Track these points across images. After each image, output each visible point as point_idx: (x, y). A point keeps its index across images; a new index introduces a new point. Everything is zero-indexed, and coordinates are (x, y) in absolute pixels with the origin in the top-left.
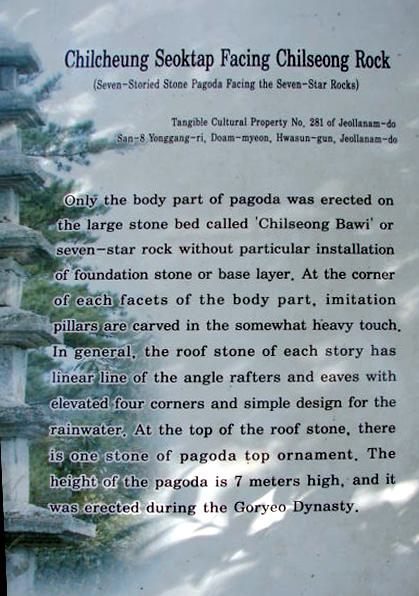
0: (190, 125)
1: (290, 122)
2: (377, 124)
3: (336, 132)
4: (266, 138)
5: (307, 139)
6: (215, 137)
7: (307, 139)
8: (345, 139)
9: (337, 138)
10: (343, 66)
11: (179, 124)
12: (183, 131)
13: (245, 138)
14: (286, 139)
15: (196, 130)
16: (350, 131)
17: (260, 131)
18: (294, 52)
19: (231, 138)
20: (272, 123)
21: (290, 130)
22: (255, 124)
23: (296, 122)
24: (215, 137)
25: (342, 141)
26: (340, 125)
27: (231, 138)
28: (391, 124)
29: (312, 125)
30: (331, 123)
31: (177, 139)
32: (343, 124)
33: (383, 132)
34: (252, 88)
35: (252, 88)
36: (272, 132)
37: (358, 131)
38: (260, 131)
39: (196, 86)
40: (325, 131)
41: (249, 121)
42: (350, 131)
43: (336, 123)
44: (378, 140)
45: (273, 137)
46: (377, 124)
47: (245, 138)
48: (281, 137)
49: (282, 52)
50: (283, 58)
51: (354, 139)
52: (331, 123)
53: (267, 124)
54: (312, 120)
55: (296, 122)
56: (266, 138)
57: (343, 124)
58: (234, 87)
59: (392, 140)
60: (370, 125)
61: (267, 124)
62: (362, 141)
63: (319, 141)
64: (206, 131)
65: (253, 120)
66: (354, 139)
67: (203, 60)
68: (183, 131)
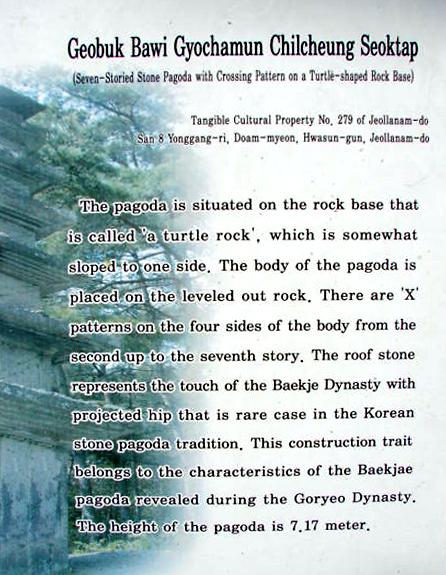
0: (210, 124)
2: (408, 121)
3: (366, 131)
4: (291, 138)
5: (336, 138)
6: (239, 138)
7: (336, 138)
8: (375, 139)
9: (366, 137)
11: (200, 123)
12: (203, 130)
13: (270, 138)
14: (314, 139)
15: (217, 130)
17: (284, 130)
19: (256, 138)
21: (317, 129)
22: (280, 122)
23: (324, 120)
24: (239, 138)
25: (372, 140)
27: (256, 138)
28: (423, 121)
29: (340, 123)
30: (361, 121)
31: (198, 140)
32: (374, 121)
33: (415, 130)
36: (298, 131)
37: (391, 130)
38: (284, 130)
40: (354, 129)
41: (274, 119)
43: (367, 120)
44: (409, 139)
45: (299, 137)
46: (408, 121)
47: (270, 138)
48: (308, 137)
52: (361, 121)
53: (293, 121)
54: (340, 117)
55: (324, 120)
56: (291, 138)
57: (374, 121)
58: (262, 79)
59: (424, 139)
60: (402, 122)
61: (293, 121)
62: (392, 140)
64: (229, 130)
67: (226, 48)
68: (203, 130)
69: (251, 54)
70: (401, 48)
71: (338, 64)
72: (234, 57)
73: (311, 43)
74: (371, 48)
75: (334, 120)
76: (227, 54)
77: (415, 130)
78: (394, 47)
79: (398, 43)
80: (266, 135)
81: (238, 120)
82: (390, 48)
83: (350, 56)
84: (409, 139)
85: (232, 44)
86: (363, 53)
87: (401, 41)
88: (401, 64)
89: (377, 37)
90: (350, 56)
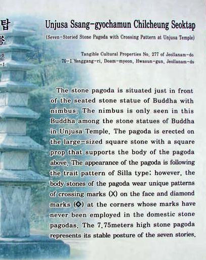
1: (142, 54)
2: (184, 55)
3: (165, 59)
8: (169, 62)
9: (165, 61)
10: (166, 28)
12: (87, 58)
16: (171, 58)
18: (141, 21)
20: (130, 54)
21: (141, 58)
23: (145, 54)
25: (167, 62)
26: (167, 56)
28: (191, 55)
30: (162, 55)
32: (168, 55)
33: (187, 58)
34: (137, 39)
35: (137, 39)
36: (133, 58)
38: (129, 58)
39: (95, 38)
40: (159, 58)
41: (119, 54)
42: (171, 58)
43: (165, 54)
44: (185, 62)
46: (184, 55)
49: (136, 22)
50: (137, 24)
51: (173, 62)
52: (162, 55)
53: (128, 55)
55: (145, 54)
57: (168, 55)
59: (192, 62)
61: (128, 55)
63: (156, 63)
65: (121, 53)
66: (173, 62)
69: (126, 27)
70: (188, 25)
71: (162, 32)
72: (142, 28)
73: (151, 23)
74: (176, 26)
75: (150, 54)
76: (116, 27)
77: (187, 58)
78: (185, 25)
79: (187, 23)
80: (119, 60)
81: (102, 54)
82: (184, 25)
83: (167, 28)
84: (185, 62)
85: (118, 23)
86: (172, 27)
87: (188, 23)
88: (187, 32)
89: (178, 21)
90: (167, 28)
